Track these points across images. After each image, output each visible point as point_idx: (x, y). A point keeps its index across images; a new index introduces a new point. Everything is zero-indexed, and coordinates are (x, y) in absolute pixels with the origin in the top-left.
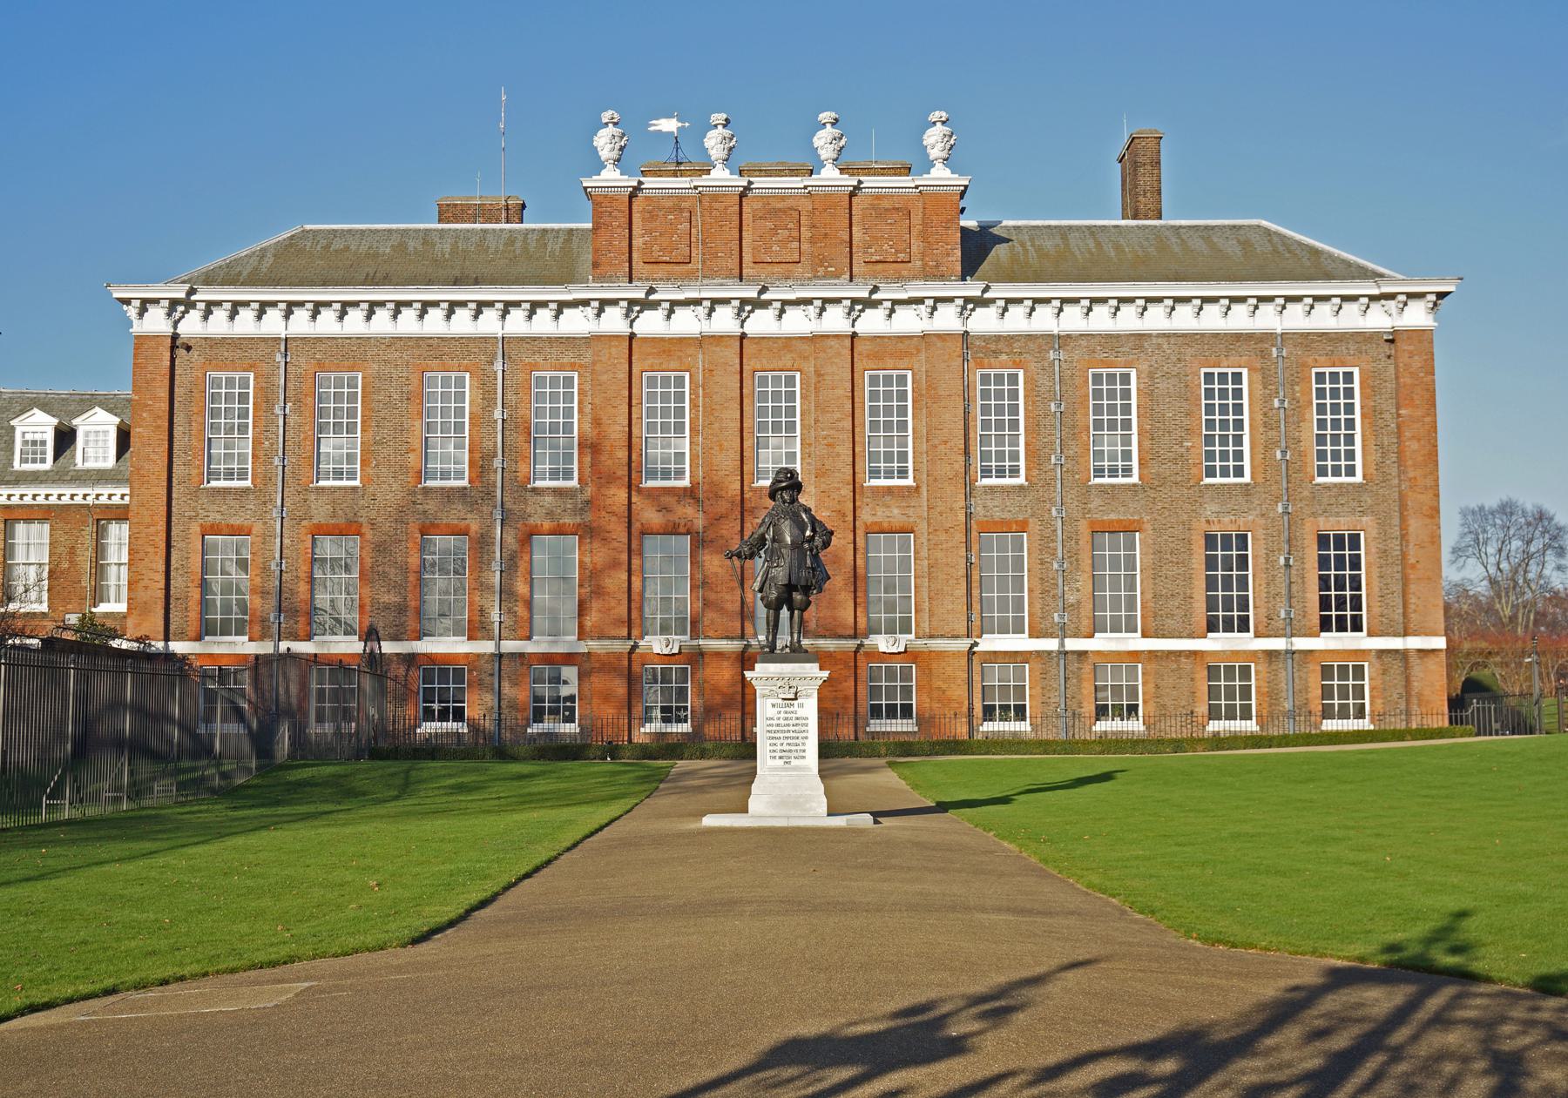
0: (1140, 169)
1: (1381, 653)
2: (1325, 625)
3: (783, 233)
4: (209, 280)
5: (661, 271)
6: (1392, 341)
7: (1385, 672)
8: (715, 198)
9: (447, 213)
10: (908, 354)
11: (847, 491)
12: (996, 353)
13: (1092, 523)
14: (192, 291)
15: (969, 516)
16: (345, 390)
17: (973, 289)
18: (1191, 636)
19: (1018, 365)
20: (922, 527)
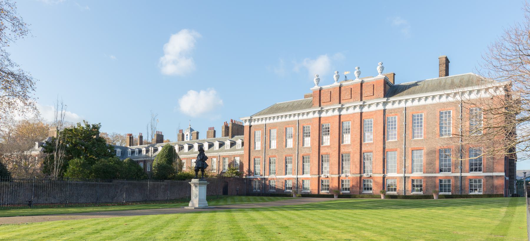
0: (446, 66)
1: (486, 177)
2: (471, 170)
3: (348, 93)
4: (256, 115)
5: (325, 104)
6: (492, 98)
7: (487, 181)
8: (334, 88)
9: (306, 96)
10: (372, 115)
11: (359, 145)
12: (391, 113)
13: (412, 148)
14: (251, 118)
15: (384, 148)
16: (274, 132)
17: (385, 100)
18: (435, 173)
19: (396, 115)
20: (374, 151)
